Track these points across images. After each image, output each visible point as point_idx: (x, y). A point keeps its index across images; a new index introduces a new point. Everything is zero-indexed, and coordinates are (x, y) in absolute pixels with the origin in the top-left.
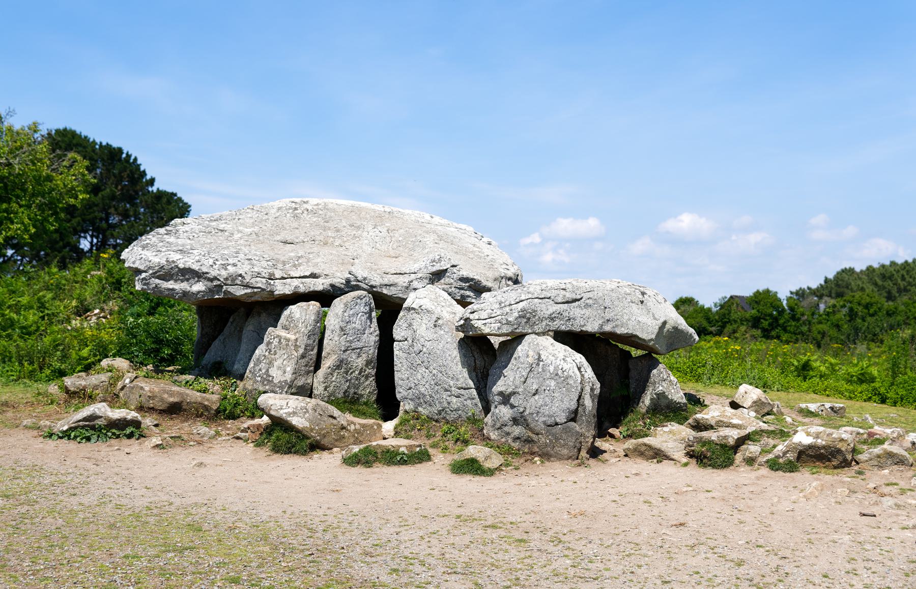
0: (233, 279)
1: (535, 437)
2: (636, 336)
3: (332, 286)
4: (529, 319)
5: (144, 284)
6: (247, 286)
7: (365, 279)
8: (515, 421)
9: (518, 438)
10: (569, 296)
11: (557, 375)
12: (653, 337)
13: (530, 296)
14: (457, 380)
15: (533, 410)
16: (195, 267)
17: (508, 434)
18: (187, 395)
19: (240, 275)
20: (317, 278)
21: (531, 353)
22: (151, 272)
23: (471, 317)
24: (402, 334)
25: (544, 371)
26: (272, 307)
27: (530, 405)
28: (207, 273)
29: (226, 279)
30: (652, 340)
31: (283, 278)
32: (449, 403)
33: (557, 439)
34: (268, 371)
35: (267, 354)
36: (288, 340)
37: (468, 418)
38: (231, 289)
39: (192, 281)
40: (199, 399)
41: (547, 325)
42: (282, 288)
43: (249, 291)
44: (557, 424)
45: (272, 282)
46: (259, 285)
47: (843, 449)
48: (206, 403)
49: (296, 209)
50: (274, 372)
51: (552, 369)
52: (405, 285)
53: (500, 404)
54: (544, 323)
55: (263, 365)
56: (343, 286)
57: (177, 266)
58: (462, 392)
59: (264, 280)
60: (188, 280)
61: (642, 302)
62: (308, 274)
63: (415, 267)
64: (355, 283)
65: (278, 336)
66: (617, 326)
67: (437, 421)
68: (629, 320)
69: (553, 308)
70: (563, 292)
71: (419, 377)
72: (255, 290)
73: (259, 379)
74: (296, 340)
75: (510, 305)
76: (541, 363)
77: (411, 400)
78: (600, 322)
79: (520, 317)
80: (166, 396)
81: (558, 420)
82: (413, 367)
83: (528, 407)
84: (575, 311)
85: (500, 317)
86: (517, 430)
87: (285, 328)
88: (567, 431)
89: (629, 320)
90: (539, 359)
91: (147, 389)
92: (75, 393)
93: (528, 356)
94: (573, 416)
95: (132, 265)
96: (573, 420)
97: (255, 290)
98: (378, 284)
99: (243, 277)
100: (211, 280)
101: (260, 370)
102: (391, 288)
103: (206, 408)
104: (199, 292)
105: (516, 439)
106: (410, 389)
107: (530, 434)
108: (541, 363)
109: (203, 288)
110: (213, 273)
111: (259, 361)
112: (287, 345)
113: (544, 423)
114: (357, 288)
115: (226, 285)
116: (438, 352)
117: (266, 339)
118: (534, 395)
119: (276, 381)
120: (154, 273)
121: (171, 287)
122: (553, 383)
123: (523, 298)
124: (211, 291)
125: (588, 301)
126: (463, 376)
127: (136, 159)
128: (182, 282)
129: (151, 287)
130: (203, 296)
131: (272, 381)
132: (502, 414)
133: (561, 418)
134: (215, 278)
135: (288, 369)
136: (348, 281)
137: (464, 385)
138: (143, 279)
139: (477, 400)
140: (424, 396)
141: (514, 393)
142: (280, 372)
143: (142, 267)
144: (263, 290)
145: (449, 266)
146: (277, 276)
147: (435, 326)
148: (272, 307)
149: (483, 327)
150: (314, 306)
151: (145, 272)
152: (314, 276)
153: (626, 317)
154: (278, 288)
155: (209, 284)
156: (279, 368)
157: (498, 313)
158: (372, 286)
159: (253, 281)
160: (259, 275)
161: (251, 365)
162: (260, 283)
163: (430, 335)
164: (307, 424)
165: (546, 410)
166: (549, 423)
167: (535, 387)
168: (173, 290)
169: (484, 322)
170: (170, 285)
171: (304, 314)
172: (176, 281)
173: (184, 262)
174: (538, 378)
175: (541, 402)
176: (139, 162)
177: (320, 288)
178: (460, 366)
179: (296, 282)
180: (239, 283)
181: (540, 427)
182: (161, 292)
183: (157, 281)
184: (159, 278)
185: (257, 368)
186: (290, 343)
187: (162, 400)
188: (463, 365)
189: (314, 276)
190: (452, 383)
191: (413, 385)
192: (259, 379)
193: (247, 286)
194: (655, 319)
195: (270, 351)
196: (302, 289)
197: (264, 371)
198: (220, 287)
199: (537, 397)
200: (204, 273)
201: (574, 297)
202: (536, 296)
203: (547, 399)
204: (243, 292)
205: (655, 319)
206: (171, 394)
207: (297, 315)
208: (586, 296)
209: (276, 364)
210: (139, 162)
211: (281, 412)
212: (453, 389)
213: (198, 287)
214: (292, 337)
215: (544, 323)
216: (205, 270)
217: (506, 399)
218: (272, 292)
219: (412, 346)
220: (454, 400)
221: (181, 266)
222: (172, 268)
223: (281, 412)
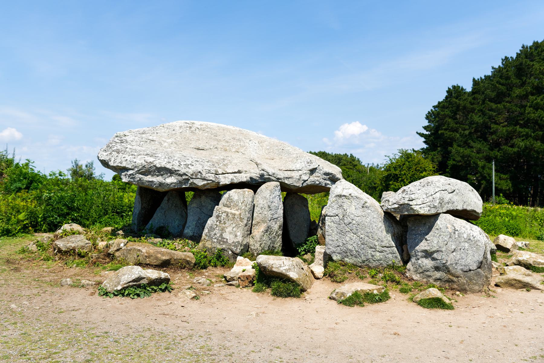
0: (197, 174)
1: (455, 279)
2: (475, 211)
3: (251, 178)
5: (132, 178)
6: (204, 179)
7: (274, 174)
8: (437, 269)
9: (440, 279)
11: (470, 239)
14: (382, 241)
15: (453, 262)
16: (169, 166)
18: (174, 254)
19: (200, 172)
20: (241, 173)
21: (449, 226)
22: (136, 169)
23: (411, 203)
24: (334, 212)
25: (459, 237)
26: (214, 193)
27: (449, 259)
28: (178, 171)
29: (192, 175)
31: (223, 174)
32: (373, 256)
33: (471, 280)
34: (221, 235)
35: (218, 223)
36: (235, 215)
37: (388, 265)
38: (196, 181)
39: (165, 176)
40: (183, 257)
42: (224, 180)
43: (205, 182)
44: (470, 270)
45: (218, 176)
46: (211, 178)
48: (188, 259)
49: (190, 128)
50: (226, 235)
51: (465, 236)
52: (298, 177)
53: (422, 257)
55: (216, 231)
56: (258, 178)
57: (155, 166)
58: (386, 249)
60: (162, 175)
62: (236, 171)
63: (298, 166)
64: (267, 177)
67: (360, 267)
71: (348, 239)
72: (209, 182)
73: (216, 240)
74: (240, 214)
76: (457, 232)
77: (339, 253)
80: (159, 255)
81: (471, 268)
82: (342, 233)
83: (449, 259)
85: (429, 203)
86: (438, 275)
87: (225, 205)
88: (478, 274)
90: (455, 230)
91: (144, 251)
92: (66, 252)
93: (447, 228)
95: (120, 165)
96: (479, 267)
97: (209, 182)
98: (282, 177)
99: (201, 173)
100: (181, 175)
101: (215, 234)
102: (290, 179)
103: (188, 262)
104: (172, 183)
105: (436, 280)
106: (338, 246)
107: (451, 277)
108: (457, 232)
109: (175, 181)
110: (183, 171)
111: (212, 229)
113: (462, 270)
114: (269, 180)
115: (192, 178)
116: (366, 224)
117: (215, 213)
118: (453, 252)
120: (138, 171)
121: (151, 180)
122: (467, 245)
123: (437, 191)
124: (180, 182)
126: (388, 239)
128: (158, 176)
129: (136, 180)
130: (175, 186)
131: (227, 242)
132: (424, 264)
133: (474, 266)
134: (185, 174)
135: (239, 234)
136: (262, 176)
137: (387, 245)
138: (130, 175)
139: (398, 254)
140: (351, 251)
141: (438, 251)
142: (232, 236)
143: (129, 166)
144: (213, 181)
146: (220, 173)
147: (363, 207)
148: (214, 193)
149: (420, 210)
150: (248, 192)
151: (132, 169)
152: (239, 172)
155: (180, 178)
156: (230, 233)
157: (428, 201)
158: (278, 179)
159: (207, 175)
161: (206, 231)
162: (211, 177)
163: (359, 212)
165: (463, 262)
166: (465, 270)
167: (453, 247)
168: (152, 182)
169: (420, 206)
170: (149, 178)
171: (241, 197)
172: (153, 176)
173: (160, 163)
174: (456, 242)
175: (458, 257)
177: (244, 180)
178: (384, 233)
179: (231, 176)
180: (200, 177)
181: (459, 272)
182: (143, 183)
183: (141, 176)
184: (141, 173)
185: (213, 233)
186: (236, 217)
187: (157, 258)
188: (387, 232)
189: (239, 172)
190: (377, 243)
192: (216, 240)
193: (204, 179)
195: (220, 221)
196: (236, 181)
197: (218, 235)
198: (188, 180)
199: (454, 254)
200: (176, 171)
203: (463, 255)
206: (163, 254)
209: (227, 230)
211: (281, 269)
212: (378, 247)
213: (171, 180)
214: (237, 213)
216: (177, 169)
217: (428, 254)
218: (219, 183)
219: (343, 219)
220: (378, 254)
221: (158, 166)
222: (150, 167)
223: (281, 269)
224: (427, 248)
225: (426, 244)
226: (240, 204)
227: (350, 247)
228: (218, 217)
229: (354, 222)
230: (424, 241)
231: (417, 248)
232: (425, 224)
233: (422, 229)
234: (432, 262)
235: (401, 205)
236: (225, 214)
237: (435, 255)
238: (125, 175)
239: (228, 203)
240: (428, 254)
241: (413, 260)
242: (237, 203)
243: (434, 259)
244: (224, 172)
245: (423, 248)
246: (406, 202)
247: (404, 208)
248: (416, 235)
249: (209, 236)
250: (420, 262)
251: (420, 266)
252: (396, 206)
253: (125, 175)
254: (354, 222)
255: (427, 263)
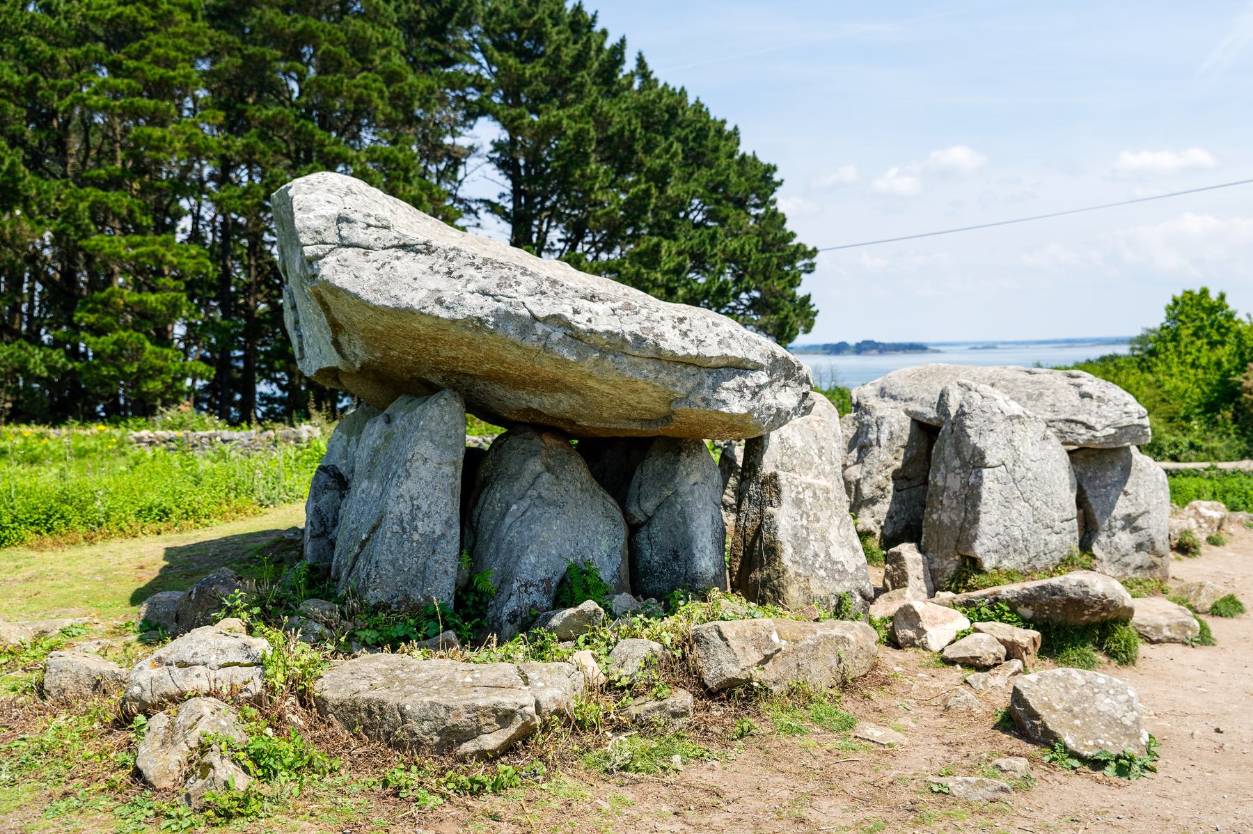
8: (1139, 547)
17: (1127, 565)
24: (1000, 456)
34: (828, 554)
55: (814, 546)
65: (809, 486)
71: (1014, 514)
101: (816, 555)
112: (828, 500)
119: (851, 569)
178: (1068, 491)
190: (1056, 516)
191: (1001, 529)
207: (798, 442)
217: (1130, 523)
224: (1131, 510)
225: (1127, 503)
226: (816, 459)
227: (1017, 533)
228: (798, 502)
229: (1030, 475)
230: (1122, 497)
231: (1115, 512)
232: (1112, 463)
233: (1113, 475)
234: (1132, 536)
235: (1120, 428)
236: (808, 493)
237: (1140, 522)
238: (740, 389)
239: (785, 459)
240: (1130, 523)
241: (1103, 538)
242: (808, 458)
243: (1136, 530)
245: (1125, 512)
246: (1136, 422)
247: (1127, 433)
248: (1105, 487)
249: (805, 566)
250: (1116, 539)
251: (1116, 548)
252: (1113, 431)
253: (740, 389)
254: (1030, 475)
255: (1125, 540)
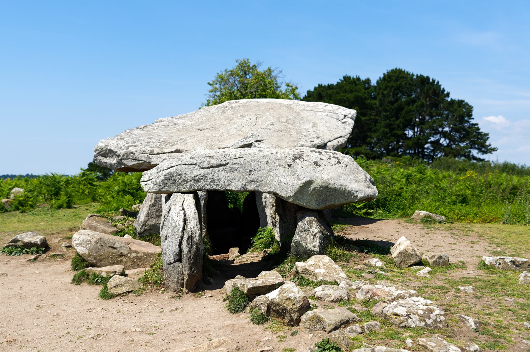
0: (127, 156)
4: (175, 181)
6: (135, 159)
10: (214, 162)
12: (292, 194)
13: (179, 163)
19: (132, 153)
20: (181, 152)
29: (124, 155)
30: (290, 197)
31: (159, 154)
41: (191, 185)
43: (136, 162)
45: (151, 156)
46: (143, 159)
47: (288, 308)
54: (189, 184)
59: (146, 155)
61: (289, 166)
62: (173, 150)
66: (260, 186)
68: (272, 180)
69: (197, 172)
70: (209, 159)
72: (140, 162)
75: (164, 170)
78: (243, 183)
79: (166, 179)
84: (221, 174)
89: (272, 180)
94: (178, 257)
97: (140, 162)
99: (134, 154)
110: (121, 152)
125: (234, 166)
127: (438, 82)
144: (145, 162)
145: (253, 141)
146: (155, 152)
153: (270, 178)
154: (153, 160)
159: (139, 156)
160: (144, 152)
164: (87, 252)
169: (145, 183)
176: (440, 84)
180: (131, 157)
184: (102, 155)
194: (299, 179)
201: (219, 162)
202: (184, 163)
204: (132, 163)
205: (299, 179)
208: (231, 162)
210: (440, 84)
215: (189, 184)
244: (160, 152)
